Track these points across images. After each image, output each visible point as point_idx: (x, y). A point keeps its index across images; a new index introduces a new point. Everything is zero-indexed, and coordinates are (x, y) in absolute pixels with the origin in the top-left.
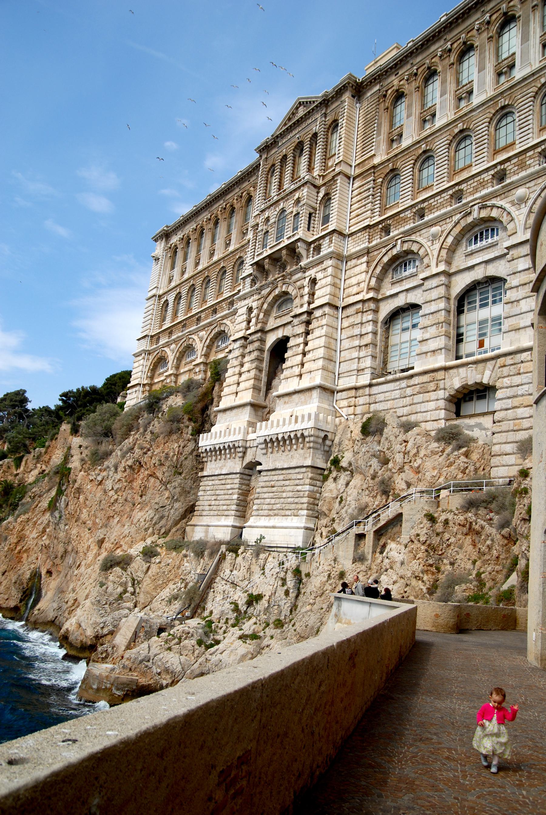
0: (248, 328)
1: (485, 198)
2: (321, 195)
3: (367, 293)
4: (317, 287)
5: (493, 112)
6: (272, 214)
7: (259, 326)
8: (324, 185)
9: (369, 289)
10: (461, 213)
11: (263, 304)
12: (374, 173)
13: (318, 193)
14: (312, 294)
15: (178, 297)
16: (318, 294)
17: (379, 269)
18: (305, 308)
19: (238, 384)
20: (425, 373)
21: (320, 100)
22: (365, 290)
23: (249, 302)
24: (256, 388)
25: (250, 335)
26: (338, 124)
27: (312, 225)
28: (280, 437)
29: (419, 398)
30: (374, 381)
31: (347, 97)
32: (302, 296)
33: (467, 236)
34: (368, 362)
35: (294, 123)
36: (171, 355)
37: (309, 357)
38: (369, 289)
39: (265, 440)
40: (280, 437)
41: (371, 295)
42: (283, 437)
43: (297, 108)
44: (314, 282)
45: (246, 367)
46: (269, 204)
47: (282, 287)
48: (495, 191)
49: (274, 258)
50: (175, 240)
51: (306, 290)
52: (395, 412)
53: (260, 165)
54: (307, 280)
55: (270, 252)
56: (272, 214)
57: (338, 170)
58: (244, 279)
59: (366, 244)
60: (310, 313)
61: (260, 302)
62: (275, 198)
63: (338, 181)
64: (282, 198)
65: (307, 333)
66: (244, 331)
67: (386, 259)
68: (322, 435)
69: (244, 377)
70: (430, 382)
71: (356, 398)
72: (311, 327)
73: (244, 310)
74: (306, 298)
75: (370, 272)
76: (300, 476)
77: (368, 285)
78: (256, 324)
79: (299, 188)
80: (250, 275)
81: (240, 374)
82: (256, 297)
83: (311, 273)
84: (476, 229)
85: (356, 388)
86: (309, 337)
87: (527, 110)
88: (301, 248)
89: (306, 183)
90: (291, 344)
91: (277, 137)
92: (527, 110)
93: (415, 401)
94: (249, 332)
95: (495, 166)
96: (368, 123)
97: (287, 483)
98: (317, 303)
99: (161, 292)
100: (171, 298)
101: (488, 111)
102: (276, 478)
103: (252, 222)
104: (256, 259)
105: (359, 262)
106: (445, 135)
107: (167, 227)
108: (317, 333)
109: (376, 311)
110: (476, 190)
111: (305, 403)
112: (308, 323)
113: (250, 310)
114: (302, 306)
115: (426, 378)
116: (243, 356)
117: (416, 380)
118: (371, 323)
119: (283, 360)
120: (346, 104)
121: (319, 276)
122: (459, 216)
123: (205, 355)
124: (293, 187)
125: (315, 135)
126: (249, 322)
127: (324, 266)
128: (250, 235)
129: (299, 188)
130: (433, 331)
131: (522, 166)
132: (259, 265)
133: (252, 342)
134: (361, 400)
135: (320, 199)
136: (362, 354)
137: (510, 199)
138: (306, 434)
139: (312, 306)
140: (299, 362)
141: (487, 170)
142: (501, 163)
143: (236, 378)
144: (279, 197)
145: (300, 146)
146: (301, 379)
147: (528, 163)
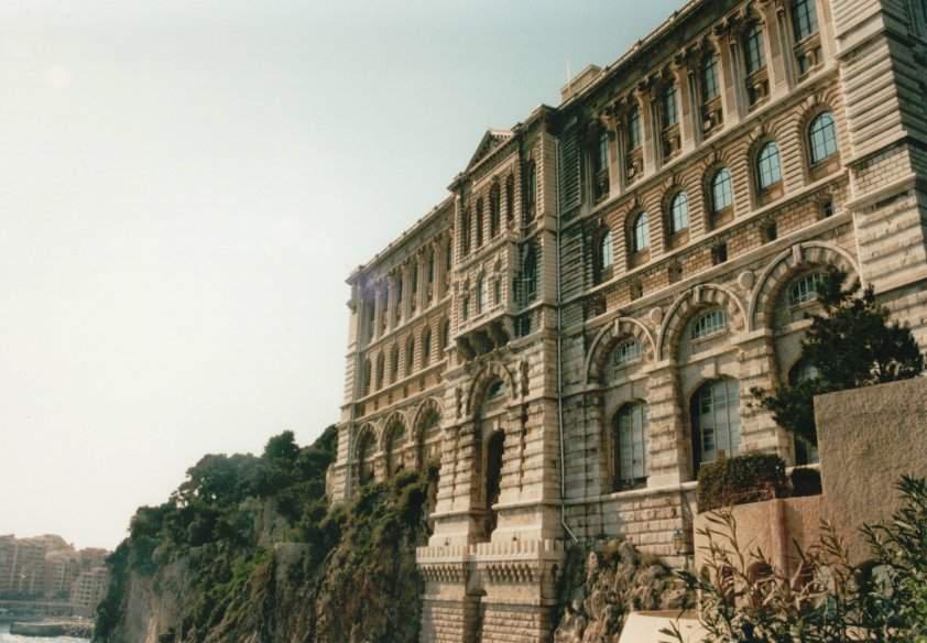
0: (459, 416)
1: (705, 280)
2: (525, 254)
3: (588, 383)
4: (530, 374)
5: (704, 167)
6: (473, 274)
7: (471, 417)
8: (527, 242)
9: (590, 379)
10: (682, 292)
11: (473, 386)
12: (583, 228)
13: (522, 251)
14: (526, 381)
15: (381, 359)
16: (532, 383)
17: (598, 353)
18: (518, 401)
19: (454, 485)
20: (661, 494)
21: (512, 134)
22: (586, 379)
23: (457, 382)
24: (473, 491)
25: (464, 424)
26: (535, 165)
27: (518, 289)
28: (503, 565)
29: (654, 525)
30: (604, 497)
31: (541, 135)
32: (514, 385)
33: (693, 319)
34: (597, 473)
35: (487, 161)
36: (379, 429)
37: (528, 462)
38: (590, 379)
39: (487, 567)
40: (503, 565)
41: (592, 387)
42: (506, 567)
43: (488, 142)
44: (525, 367)
45: (462, 465)
46: (467, 262)
47: (492, 369)
48: (716, 271)
49: (479, 334)
50: (371, 282)
51: (518, 376)
52: (631, 539)
53: (453, 204)
54: (519, 363)
55: (475, 326)
56: (473, 274)
57: (540, 226)
58: (450, 351)
59: (581, 324)
60: (525, 406)
61: (470, 383)
62: (474, 258)
63: (542, 240)
64: (482, 258)
65: (524, 432)
66: (455, 419)
67: (605, 341)
68: (550, 566)
69: (460, 477)
70: (665, 506)
71: (586, 515)
72: (527, 425)
73: (451, 392)
74: (520, 387)
75: (589, 357)
76: (529, 617)
77: (589, 373)
78: (468, 412)
79: (498, 248)
80: (454, 349)
81: (455, 473)
82: (463, 378)
83: (521, 357)
84: (702, 313)
85: (586, 505)
86: (527, 438)
87: (741, 169)
88: (508, 326)
89: (505, 243)
90: (510, 441)
91: (470, 175)
92: (741, 169)
93: (651, 528)
94: (461, 421)
95: (713, 237)
96: (569, 164)
97: (516, 622)
98: (533, 395)
99: (363, 349)
100: (373, 357)
101: (698, 165)
102: (503, 614)
103: (454, 278)
104: (460, 333)
105: (575, 342)
106: (655, 189)
107: (361, 267)
108: (536, 434)
109: (602, 404)
110: (695, 266)
111: (528, 522)
112: (524, 418)
113: (459, 392)
114: (515, 396)
115: (662, 501)
116: (456, 450)
117: (648, 503)
118: (596, 421)
119: (500, 464)
120: (541, 142)
121: (532, 360)
122: (681, 297)
123: (417, 437)
124: (491, 246)
125: (511, 177)
126: (460, 407)
127: (534, 349)
128: (452, 292)
129: (498, 248)
130: (665, 440)
131: (744, 243)
132: (462, 340)
133: (464, 434)
134: (593, 520)
135: (524, 258)
136: (589, 460)
137: (733, 282)
138: (531, 565)
139: (527, 399)
140: (517, 469)
141: (706, 242)
142: (721, 235)
143: (451, 477)
144: (478, 257)
145: (495, 188)
146: (521, 490)
147: (749, 238)
